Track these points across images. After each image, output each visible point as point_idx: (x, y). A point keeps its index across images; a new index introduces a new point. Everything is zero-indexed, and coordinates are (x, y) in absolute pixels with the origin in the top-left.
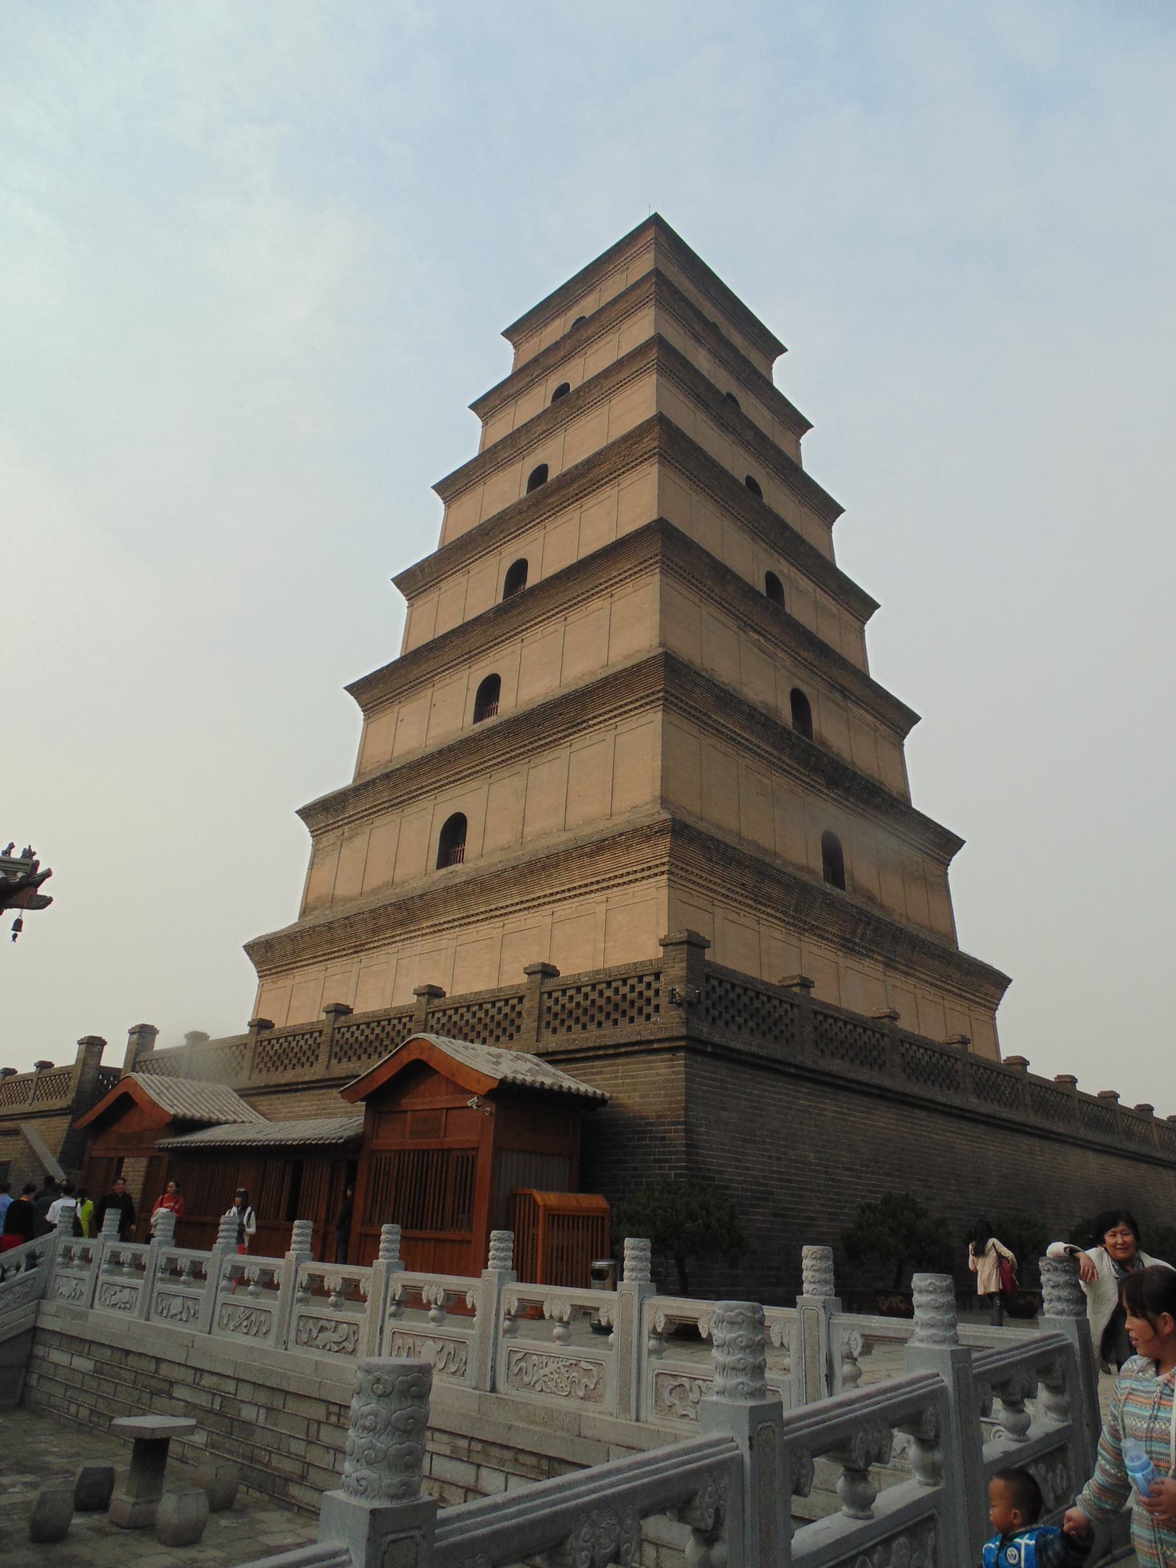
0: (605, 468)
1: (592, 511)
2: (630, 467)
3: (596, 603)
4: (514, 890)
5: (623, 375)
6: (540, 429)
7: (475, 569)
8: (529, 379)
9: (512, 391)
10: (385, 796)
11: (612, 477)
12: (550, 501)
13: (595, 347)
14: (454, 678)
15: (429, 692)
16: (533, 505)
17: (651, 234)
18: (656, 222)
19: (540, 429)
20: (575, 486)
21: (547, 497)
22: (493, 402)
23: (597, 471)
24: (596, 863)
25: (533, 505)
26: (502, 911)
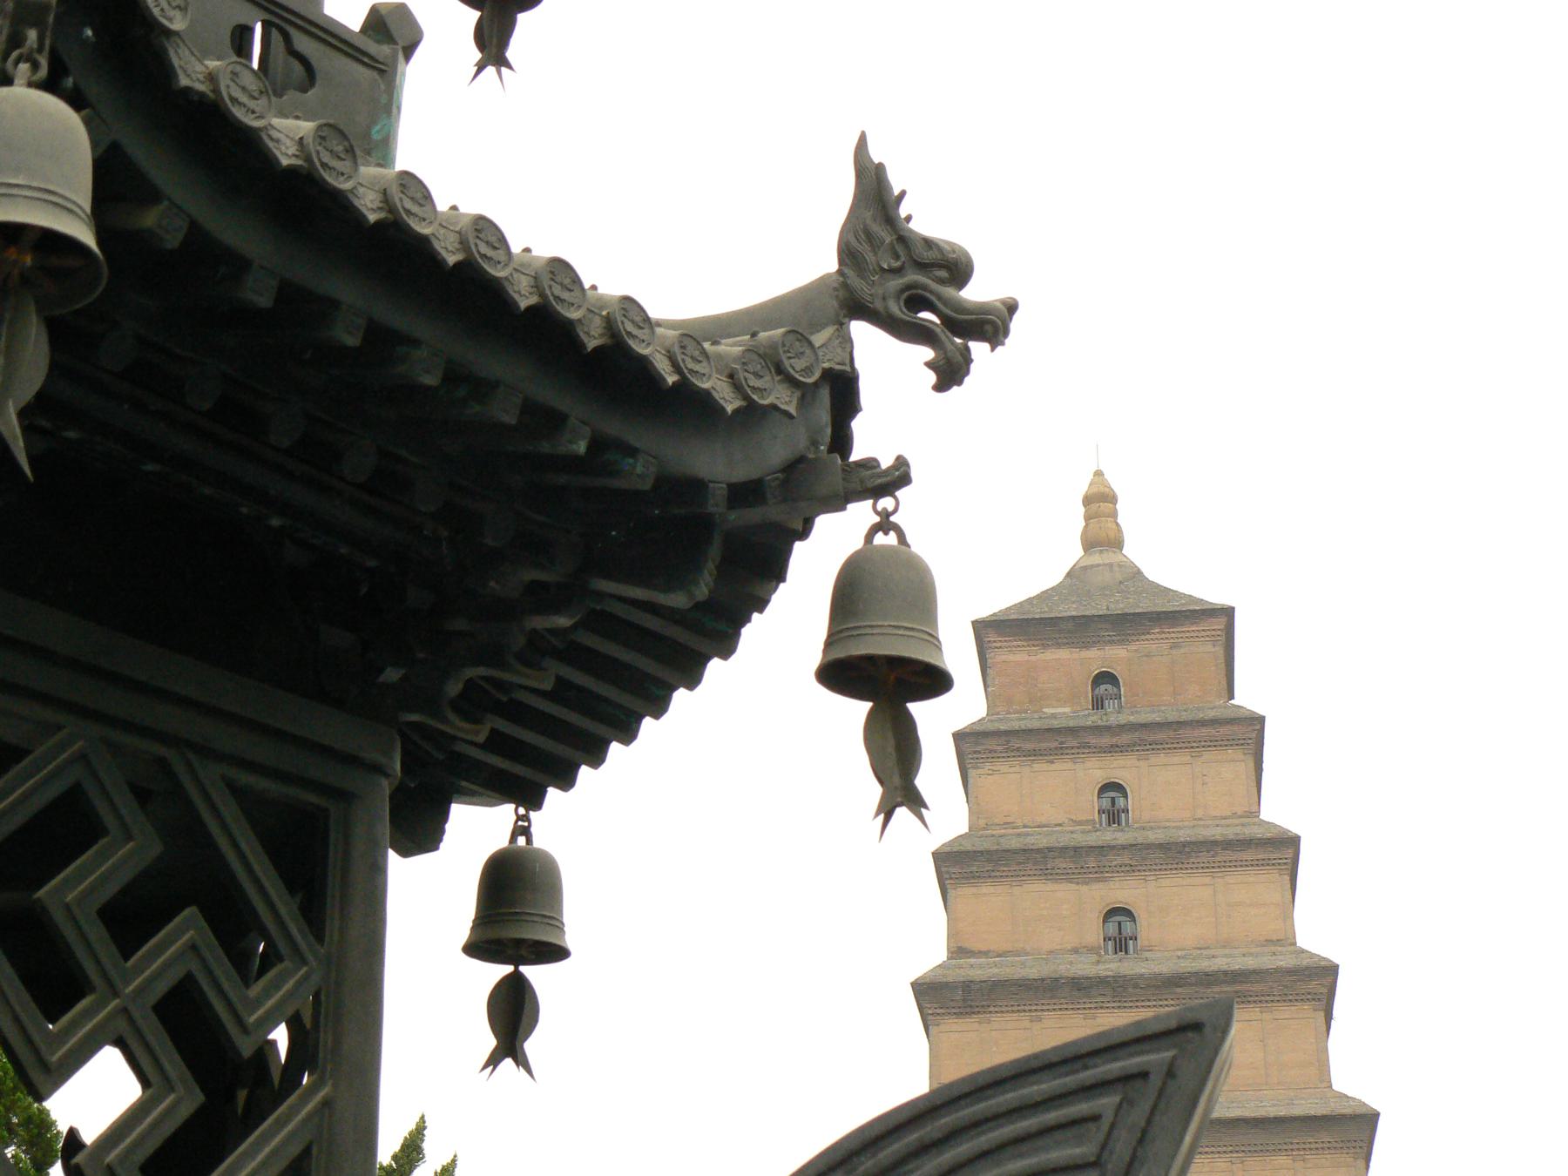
0: (1257, 987)
3: (1282, 1160)
5: (1248, 855)
6: (1119, 860)
8: (1056, 744)
9: (1029, 746)
12: (1179, 990)
13: (1162, 758)
17: (1219, 623)
18: (1228, 613)
19: (1119, 860)
22: (991, 744)
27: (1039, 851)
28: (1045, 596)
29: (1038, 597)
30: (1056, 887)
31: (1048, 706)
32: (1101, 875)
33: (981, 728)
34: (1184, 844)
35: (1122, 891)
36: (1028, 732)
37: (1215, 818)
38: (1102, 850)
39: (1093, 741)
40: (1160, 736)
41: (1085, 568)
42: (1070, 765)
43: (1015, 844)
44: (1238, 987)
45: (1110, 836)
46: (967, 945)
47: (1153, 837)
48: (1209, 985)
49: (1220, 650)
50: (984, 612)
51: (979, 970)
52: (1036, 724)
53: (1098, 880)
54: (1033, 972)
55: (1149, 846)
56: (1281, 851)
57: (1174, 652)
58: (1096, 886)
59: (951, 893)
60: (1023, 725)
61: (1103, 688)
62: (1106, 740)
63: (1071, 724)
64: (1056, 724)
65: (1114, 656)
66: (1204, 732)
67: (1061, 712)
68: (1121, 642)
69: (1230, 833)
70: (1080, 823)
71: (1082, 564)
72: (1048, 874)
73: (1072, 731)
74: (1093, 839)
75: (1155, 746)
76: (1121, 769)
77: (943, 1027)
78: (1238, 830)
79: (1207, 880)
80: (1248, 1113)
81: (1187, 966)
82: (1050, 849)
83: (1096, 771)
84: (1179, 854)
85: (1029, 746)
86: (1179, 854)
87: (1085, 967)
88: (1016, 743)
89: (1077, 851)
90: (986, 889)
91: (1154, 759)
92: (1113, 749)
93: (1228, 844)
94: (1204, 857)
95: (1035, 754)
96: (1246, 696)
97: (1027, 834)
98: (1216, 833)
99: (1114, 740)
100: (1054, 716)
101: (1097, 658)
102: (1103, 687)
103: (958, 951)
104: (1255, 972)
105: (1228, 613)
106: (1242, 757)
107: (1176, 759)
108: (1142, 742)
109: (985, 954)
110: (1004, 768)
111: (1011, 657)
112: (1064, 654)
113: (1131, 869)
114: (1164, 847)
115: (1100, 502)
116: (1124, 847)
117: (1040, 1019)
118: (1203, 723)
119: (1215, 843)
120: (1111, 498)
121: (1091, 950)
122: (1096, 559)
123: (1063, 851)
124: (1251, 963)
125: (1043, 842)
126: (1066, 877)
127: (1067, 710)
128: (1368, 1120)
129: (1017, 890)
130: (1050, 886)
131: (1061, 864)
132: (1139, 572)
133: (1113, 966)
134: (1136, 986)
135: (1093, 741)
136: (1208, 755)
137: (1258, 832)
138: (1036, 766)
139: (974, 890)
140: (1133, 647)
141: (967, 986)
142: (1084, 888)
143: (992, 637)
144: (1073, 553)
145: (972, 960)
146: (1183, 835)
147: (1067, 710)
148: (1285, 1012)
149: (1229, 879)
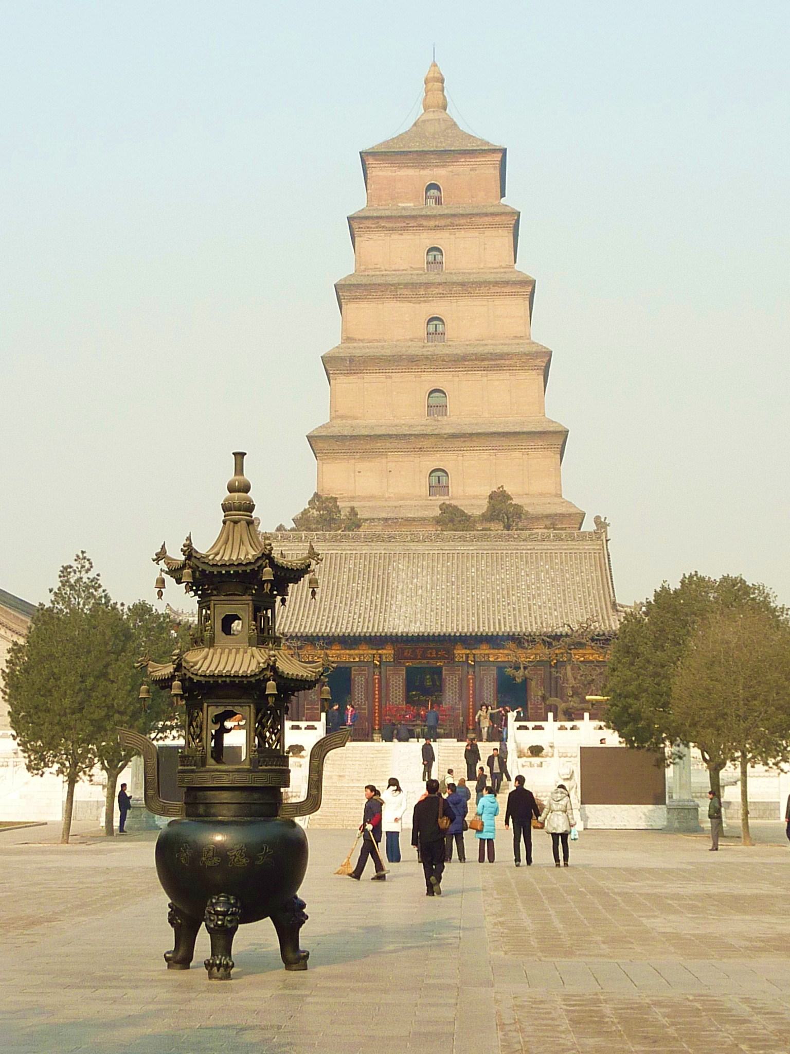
0: (507, 362)
1: (496, 383)
2: (522, 368)
3: (517, 454)
5: (507, 290)
6: (437, 291)
7: (397, 377)
9: (388, 225)
11: (510, 368)
13: (462, 233)
14: (406, 459)
15: (384, 460)
19: (437, 291)
20: (486, 363)
22: (368, 223)
23: (503, 361)
27: (392, 285)
28: (400, 138)
29: (397, 138)
30: (402, 305)
31: (401, 202)
32: (426, 299)
33: (362, 214)
34: (473, 283)
35: (438, 308)
36: (388, 218)
37: (490, 268)
38: (428, 285)
40: (462, 221)
41: (424, 121)
42: (411, 237)
43: (379, 281)
44: (498, 362)
45: (433, 277)
46: (350, 336)
47: (455, 278)
48: (483, 360)
49: (497, 173)
50: (367, 146)
51: (358, 350)
52: (394, 213)
53: (425, 301)
54: (388, 352)
55: (454, 283)
56: (527, 288)
57: (472, 172)
58: (423, 305)
59: (344, 306)
60: (388, 213)
61: (433, 192)
62: (432, 223)
63: (414, 213)
64: (404, 213)
65: (438, 174)
66: (487, 219)
67: (408, 205)
68: (443, 166)
69: (498, 277)
70: (415, 269)
71: (423, 118)
72: (396, 297)
73: (414, 217)
74: (423, 279)
75: (459, 227)
76: (442, 239)
77: (338, 381)
78: (502, 275)
79: (484, 303)
80: (500, 430)
81: (471, 350)
82: (399, 284)
83: (427, 239)
84: (468, 287)
85: (388, 225)
86: (468, 287)
87: (415, 349)
89: (414, 286)
90: (364, 305)
91: (458, 234)
92: (437, 228)
93: (496, 284)
94: (484, 290)
95: (393, 229)
96: (510, 201)
97: (387, 275)
98: (491, 278)
99: (437, 223)
100: (404, 208)
101: (429, 175)
102: (432, 191)
103: (348, 339)
104: (508, 354)
105: (504, 151)
106: (506, 234)
107: (470, 235)
108: (452, 225)
109: (362, 341)
110: (375, 237)
111: (381, 173)
112: (411, 172)
113: (442, 296)
114: (463, 284)
115: (435, 81)
116: (440, 284)
117: (391, 377)
118: (486, 215)
119: (490, 283)
120: (442, 81)
121: (421, 339)
122: (431, 116)
123: (406, 285)
124: (506, 349)
125: (396, 281)
126: (406, 299)
127: (412, 204)
128: (563, 435)
129: (380, 306)
130: (399, 304)
131: (405, 292)
132: (455, 124)
133: (431, 349)
135: (425, 223)
136: (488, 232)
137: (513, 277)
138: (393, 237)
139: (357, 305)
140: (450, 168)
141: (352, 359)
142: (417, 306)
143: (370, 161)
144: (417, 111)
145: (355, 345)
146: (472, 278)
147: (412, 204)
148: (522, 375)
149: (497, 302)
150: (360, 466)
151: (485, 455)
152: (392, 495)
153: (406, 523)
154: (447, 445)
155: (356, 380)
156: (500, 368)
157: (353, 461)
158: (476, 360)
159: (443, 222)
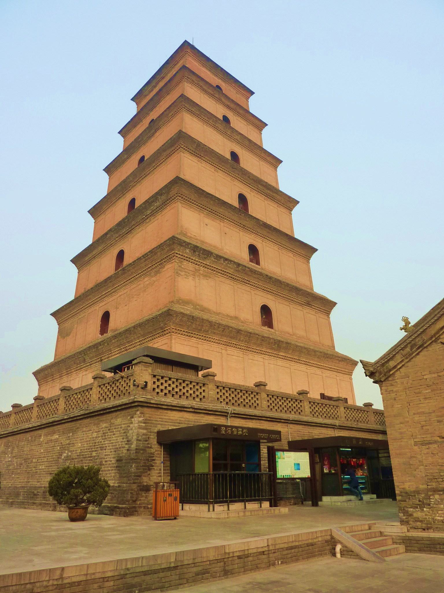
0: (278, 197)
1: (272, 207)
3: (291, 254)
4: (316, 359)
5: (268, 158)
6: (236, 137)
8: (212, 93)
10: (231, 271)
12: (260, 186)
13: (239, 119)
14: (235, 229)
15: (222, 224)
16: (254, 180)
19: (236, 137)
21: (260, 184)
24: (339, 363)
25: (254, 180)
26: (310, 364)
39: (223, 100)
44: (274, 195)
48: (269, 189)
77: (185, 155)
88: (201, 83)
91: (237, 118)
99: (229, 104)
111: (193, 61)
113: (238, 143)
130: (215, 132)
134: (249, 177)
135: (223, 100)
142: (225, 139)
150: (207, 221)
151: (276, 247)
152: (228, 251)
153: (250, 273)
154: (259, 230)
155: (196, 161)
156: (273, 199)
157: (202, 215)
158: (265, 186)
159: (232, 105)
